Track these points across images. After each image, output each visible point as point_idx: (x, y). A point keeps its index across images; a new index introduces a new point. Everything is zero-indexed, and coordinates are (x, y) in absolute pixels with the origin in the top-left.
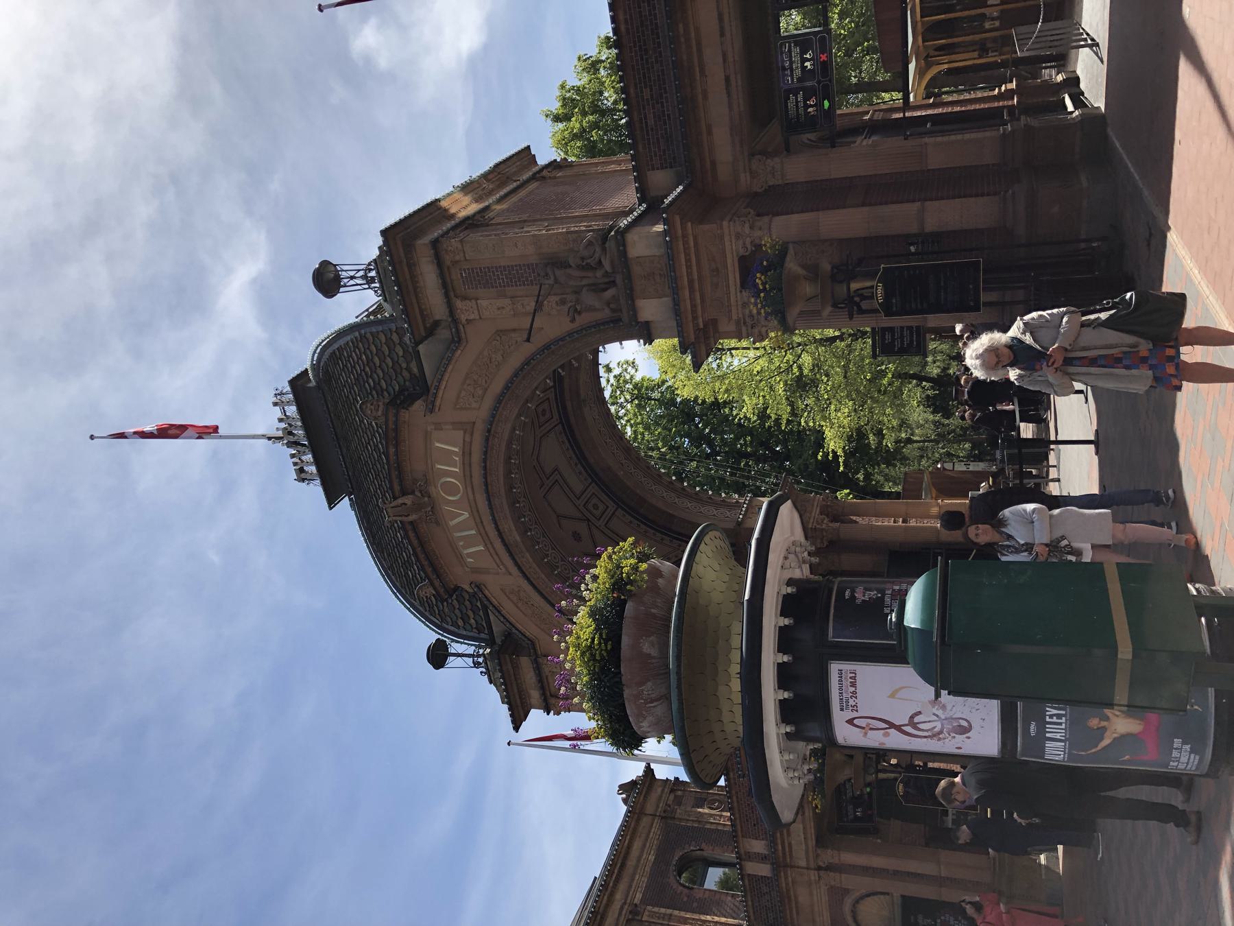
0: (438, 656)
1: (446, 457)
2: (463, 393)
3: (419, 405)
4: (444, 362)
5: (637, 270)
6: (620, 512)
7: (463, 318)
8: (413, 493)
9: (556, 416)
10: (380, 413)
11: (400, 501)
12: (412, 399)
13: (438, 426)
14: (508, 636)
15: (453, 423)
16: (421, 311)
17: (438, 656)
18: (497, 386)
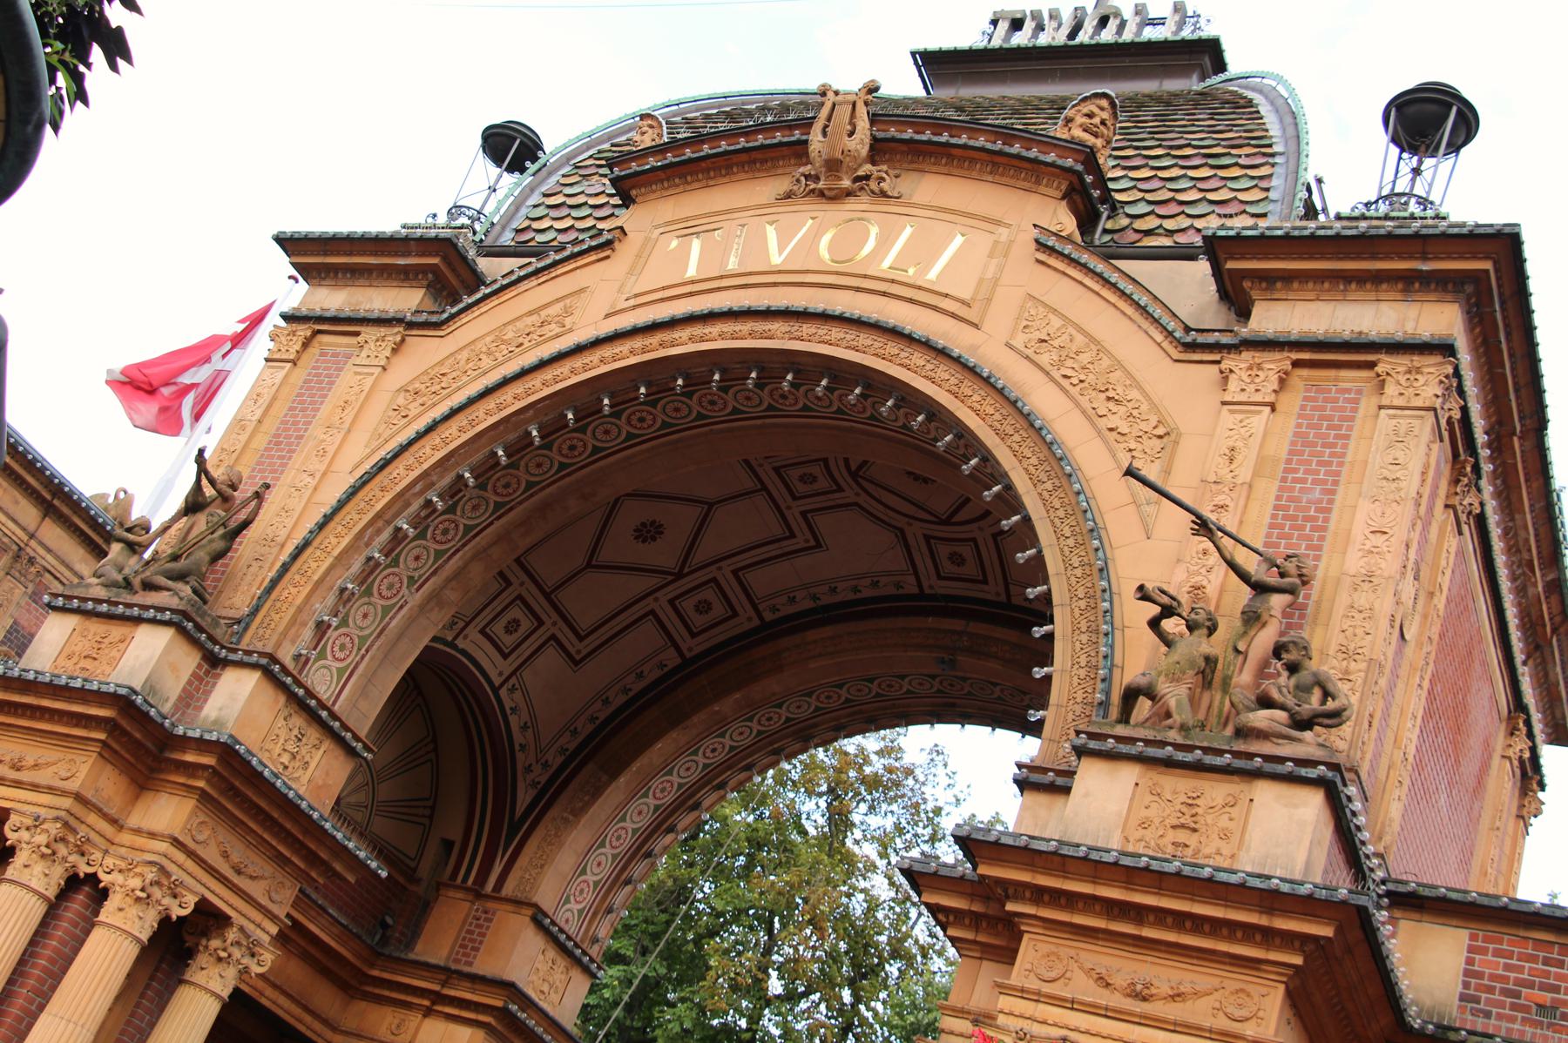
0: (510, 146)
1: (923, 252)
2: (1056, 322)
3: (1067, 222)
4: (1146, 310)
5: (1216, 791)
6: (672, 659)
7: (1238, 363)
8: (873, 158)
9: (943, 588)
10: (1078, 133)
11: (863, 123)
12: (1087, 222)
13: (1001, 251)
14: (477, 280)
15: (996, 282)
16: (1288, 278)
17: (510, 146)
18: (1044, 400)
